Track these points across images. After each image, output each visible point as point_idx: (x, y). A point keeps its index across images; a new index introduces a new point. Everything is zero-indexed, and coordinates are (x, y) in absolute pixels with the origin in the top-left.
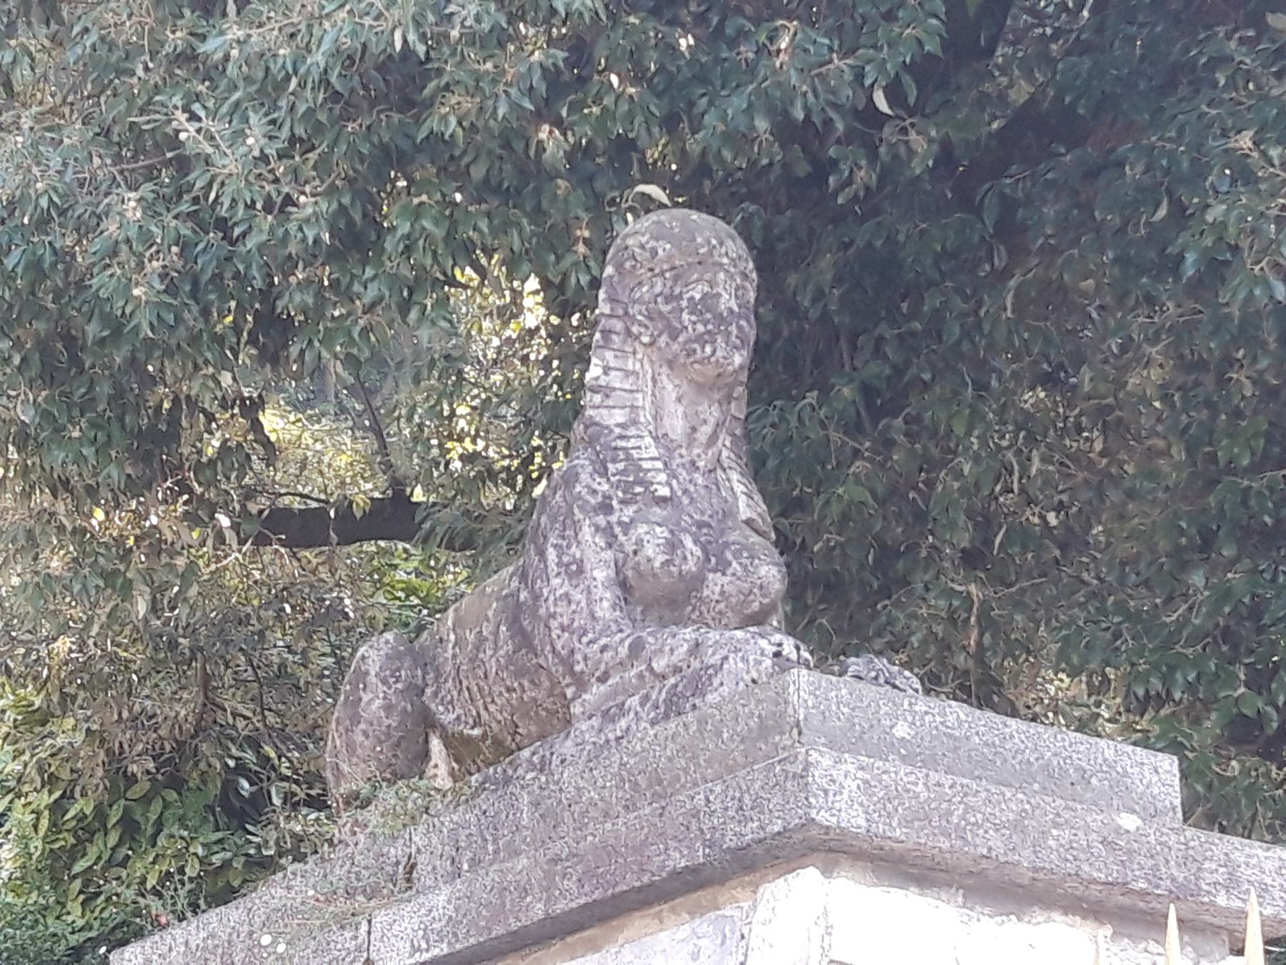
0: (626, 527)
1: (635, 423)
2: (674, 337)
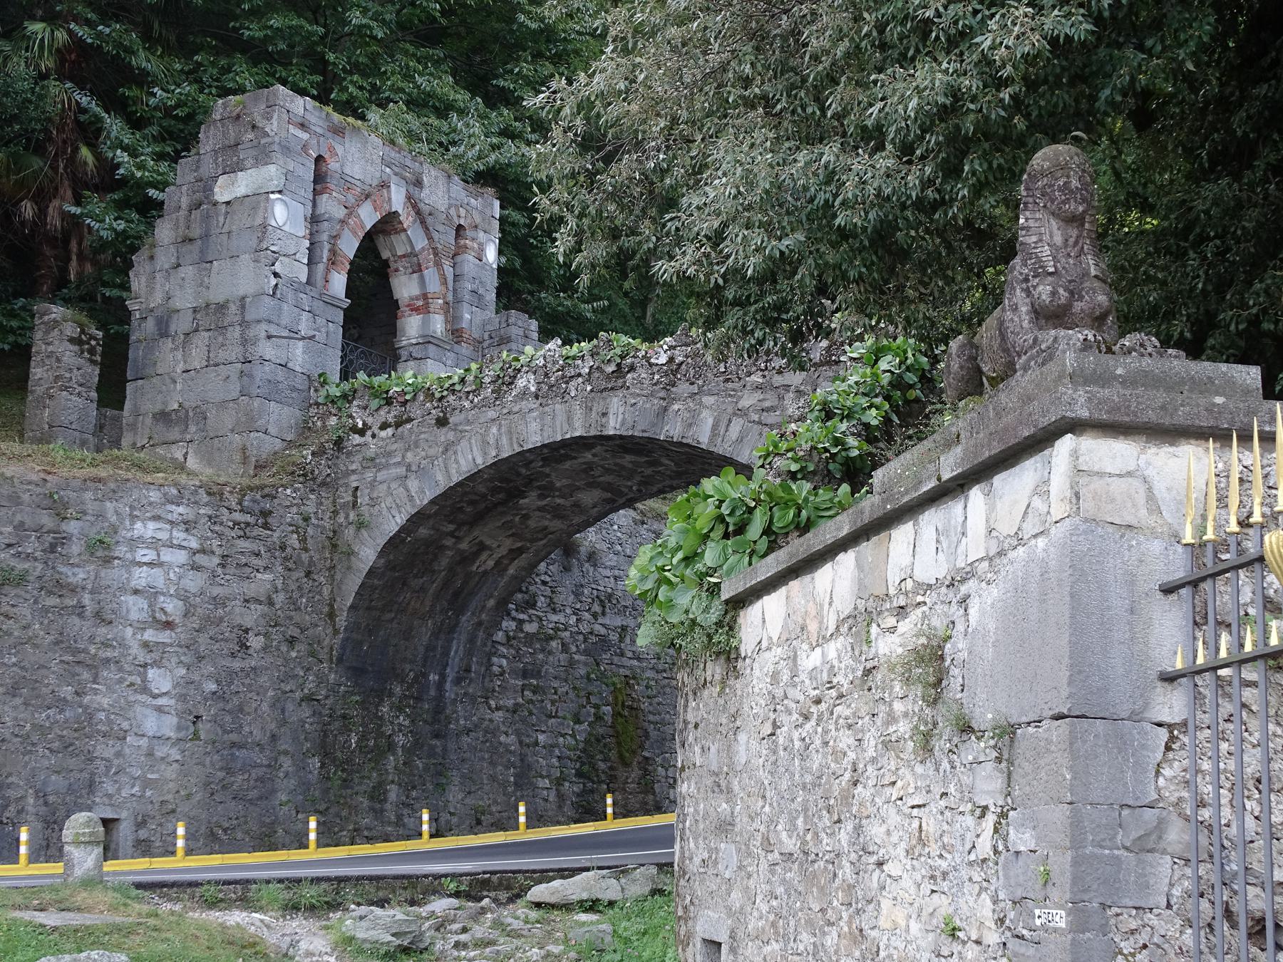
0: (1035, 287)
1: (1041, 240)
2: (1053, 203)
